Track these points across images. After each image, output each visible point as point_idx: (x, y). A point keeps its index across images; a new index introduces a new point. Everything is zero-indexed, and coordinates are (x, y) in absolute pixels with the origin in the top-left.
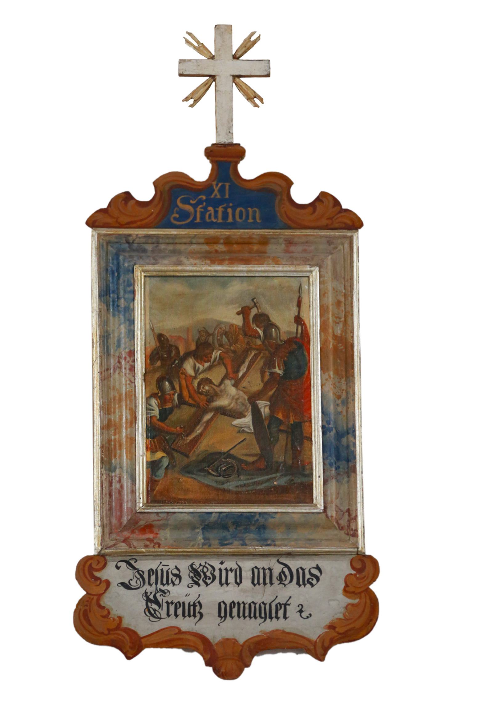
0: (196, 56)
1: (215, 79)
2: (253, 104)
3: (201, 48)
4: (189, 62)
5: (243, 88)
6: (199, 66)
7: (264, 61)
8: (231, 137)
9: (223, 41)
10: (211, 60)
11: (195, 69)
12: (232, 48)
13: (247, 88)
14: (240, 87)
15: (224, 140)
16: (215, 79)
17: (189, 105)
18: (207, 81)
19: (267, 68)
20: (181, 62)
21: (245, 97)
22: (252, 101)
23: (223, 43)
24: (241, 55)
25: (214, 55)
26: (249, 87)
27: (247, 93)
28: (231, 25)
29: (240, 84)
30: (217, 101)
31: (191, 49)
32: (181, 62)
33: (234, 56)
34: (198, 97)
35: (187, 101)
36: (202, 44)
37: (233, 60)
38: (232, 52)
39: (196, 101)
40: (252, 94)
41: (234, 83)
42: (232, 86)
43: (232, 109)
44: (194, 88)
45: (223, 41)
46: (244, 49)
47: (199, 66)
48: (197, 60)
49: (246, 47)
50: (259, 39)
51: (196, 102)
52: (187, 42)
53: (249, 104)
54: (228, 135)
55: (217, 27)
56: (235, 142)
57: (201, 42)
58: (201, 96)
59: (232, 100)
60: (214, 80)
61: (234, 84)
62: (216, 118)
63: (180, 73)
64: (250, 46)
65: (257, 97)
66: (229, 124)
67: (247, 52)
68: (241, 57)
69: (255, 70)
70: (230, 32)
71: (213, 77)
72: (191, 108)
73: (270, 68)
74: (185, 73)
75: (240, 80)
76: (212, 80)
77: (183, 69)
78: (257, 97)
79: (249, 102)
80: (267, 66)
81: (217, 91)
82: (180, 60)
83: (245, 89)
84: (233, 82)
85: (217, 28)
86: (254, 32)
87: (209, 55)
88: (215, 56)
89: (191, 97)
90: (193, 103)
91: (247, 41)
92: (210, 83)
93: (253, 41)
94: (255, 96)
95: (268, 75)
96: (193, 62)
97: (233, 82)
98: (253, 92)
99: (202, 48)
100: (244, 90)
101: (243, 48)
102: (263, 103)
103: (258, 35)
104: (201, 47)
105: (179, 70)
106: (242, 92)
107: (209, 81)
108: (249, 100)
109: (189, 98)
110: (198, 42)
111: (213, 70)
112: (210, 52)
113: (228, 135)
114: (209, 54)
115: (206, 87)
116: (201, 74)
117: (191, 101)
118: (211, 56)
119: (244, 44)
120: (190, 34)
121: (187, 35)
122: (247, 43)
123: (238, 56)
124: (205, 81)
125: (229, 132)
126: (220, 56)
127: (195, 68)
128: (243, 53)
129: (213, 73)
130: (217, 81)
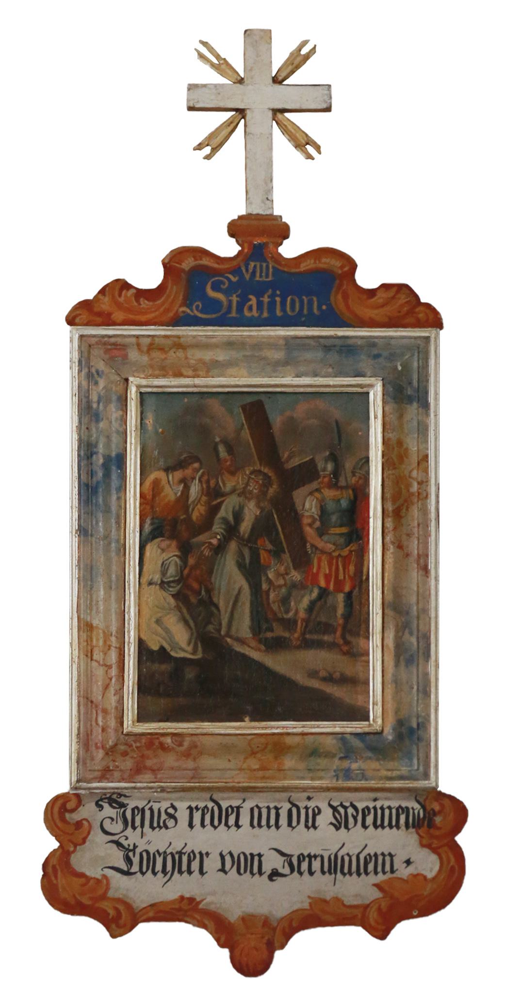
0: (214, 78)
1: (244, 114)
2: (304, 154)
3: (222, 66)
4: (204, 88)
5: (288, 130)
6: (219, 94)
7: (321, 87)
8: (270, 207)
9: (258, 56)
10: (238, 85)
11: (212, 100)
12: (271, 67)
13: (295, 130)
14: (284, 127)
15: (257, 210)
16: (244, 114)
17: (203, 157)
18: (231, 119)
19: (326, 98)
20: (192, 87)
21: (292, 142)
22: (302, 150)
23: (257, 57)
24: (285, 77)
25: (243, 77)
26: (298, 127)
27: (296, 137)
28: (271, 30)
29: (285, 123)
30: (248, 149)
31: (207, 68)
32: (192, 87)
33: (275, 78)
34: (218, 144)
35: (200, 149)
36: (225, 59)
37: (273, 85)
38: (271, 72)
39: (215, 150)
40: (303, 139)
41: (274, 122)
42: (272, 126)
43: (272, 162)
44: (212, 129)
45: (258, 56)
46: (290, 68)
47: (219, 94)
48: (216, 86)
49: (293, 64)
50: (314, 52)
51: (215, 151)
52: (201, 56)
53: (297, 155)
54: (265, 204)
55: (247, 33)
56: (275, 214)
57: (223, 57)
58: (222, 142)
59: (271, 149)
60: (244, 117)
61: (274, 122)
62: (246, 176)
63: (189, 105)
64: (300, 62)
65: (311, 144)
66: (267, 185)
67: (295, 72)
68: (286, 80)
69: (307, 100)
70: (269, 41)
71: (241, 112)
72: (206, 160)
73: (331, 98)
74: (197, 106)
75: (284, 116)
76: (240, 116)
77: (194, 100)
78: (311, 144)
79: (298, 150)
80: (327, 95)
81: (247, 133)
82: (189, 85)
83: (293, 131)
84: (274, 119)
85: (248, 35)
86: (306, 41)
87: (235, 77)
88: (245, 79)
89: (207, 143)
90: (210, 153)
91: (296, 55)
92: (237, 121)
93: (304, 55)
94: (307, 141)
95: (328, 109)
96: (210, 89)
97: (274, 119)
98: (304, 136)
99: (223, 67)
100: (291, 132)
101: (288, 66)
102: (320, 153)
103: (313, 46)
104: (222, 64)
105: (188, 101)
106: (286, 135)
107: (236, 117)
108: (298, 148)
109: (204, 145)
110: (218, 56)
111: (242, 101)
112: (239, 75)
113: (265, 204)
114: (236, 76)
115: (229, 128)
116: (222, 107)
117: (207, 150)
118: (239, 78)
119: (291, 59)
120: (205, 44)
121: (201, 45)
122: (295, 59)
123: (280, 78)
124: (229, 119)
125: (267, 199)
126: (252, 78)
127: (213, 97)
128: (289, 73)
129: (241, 107)
130: (248, 118)
